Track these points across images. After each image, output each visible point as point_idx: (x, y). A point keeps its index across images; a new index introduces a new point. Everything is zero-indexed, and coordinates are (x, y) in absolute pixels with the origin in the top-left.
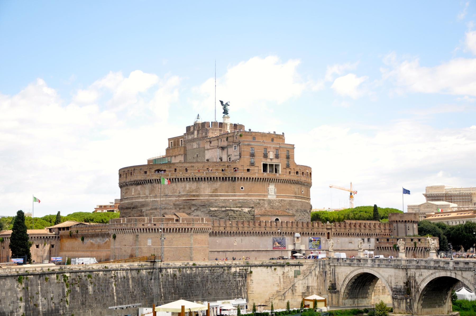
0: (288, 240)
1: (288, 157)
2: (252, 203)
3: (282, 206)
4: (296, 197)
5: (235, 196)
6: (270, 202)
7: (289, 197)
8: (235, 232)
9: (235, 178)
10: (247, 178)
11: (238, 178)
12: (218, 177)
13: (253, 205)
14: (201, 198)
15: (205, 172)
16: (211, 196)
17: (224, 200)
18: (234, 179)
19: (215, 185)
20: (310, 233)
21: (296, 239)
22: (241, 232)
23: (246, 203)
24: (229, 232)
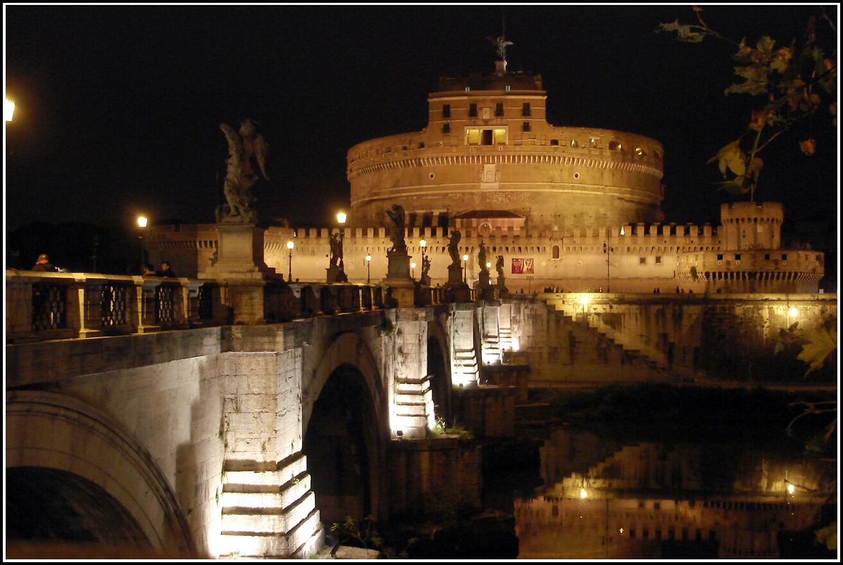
4: (553, 187)
5: (421, 190)
6: (484, 196)
9: (419, 160)
14: (382, 197)
15: (383, 155)
16: (392, 192)
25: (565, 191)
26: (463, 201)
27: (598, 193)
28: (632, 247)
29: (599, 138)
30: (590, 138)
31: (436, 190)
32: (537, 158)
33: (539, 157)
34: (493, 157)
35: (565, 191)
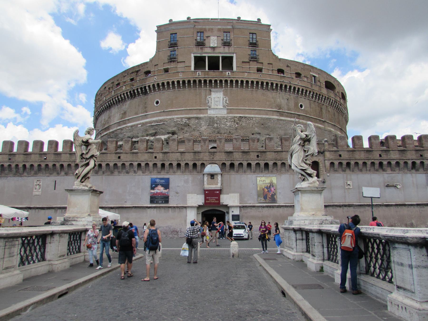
0: (186, 182)
1: (254, 45)
2: (173, 124)
3: (242, 128)
5: (146, 117)
6: (211, 121)
7: (259, 112)
8: (36, 165)
9: (145, 87)
10: (163, 84)
11: (149, 86)
12: (125, 92)
13: (174, 129)
14: (111, 131)
15: (113, 92)
17: (132, 126)
18: (144, 91)
19: (124, 107)
20: (253, 164)
21: (206, 178)
22: (51, 165)
23: (163, 126)
24: (21, 165)
25: (292, 119)
26: (189, 125)
27: (320, 126)
28: (418, 162)
29: (317, 76)
30: (311, 73)
31: (161, 116)
32: (265, 84)
33: (267, 83)
34: (221, 81)
35: (292, 119)
